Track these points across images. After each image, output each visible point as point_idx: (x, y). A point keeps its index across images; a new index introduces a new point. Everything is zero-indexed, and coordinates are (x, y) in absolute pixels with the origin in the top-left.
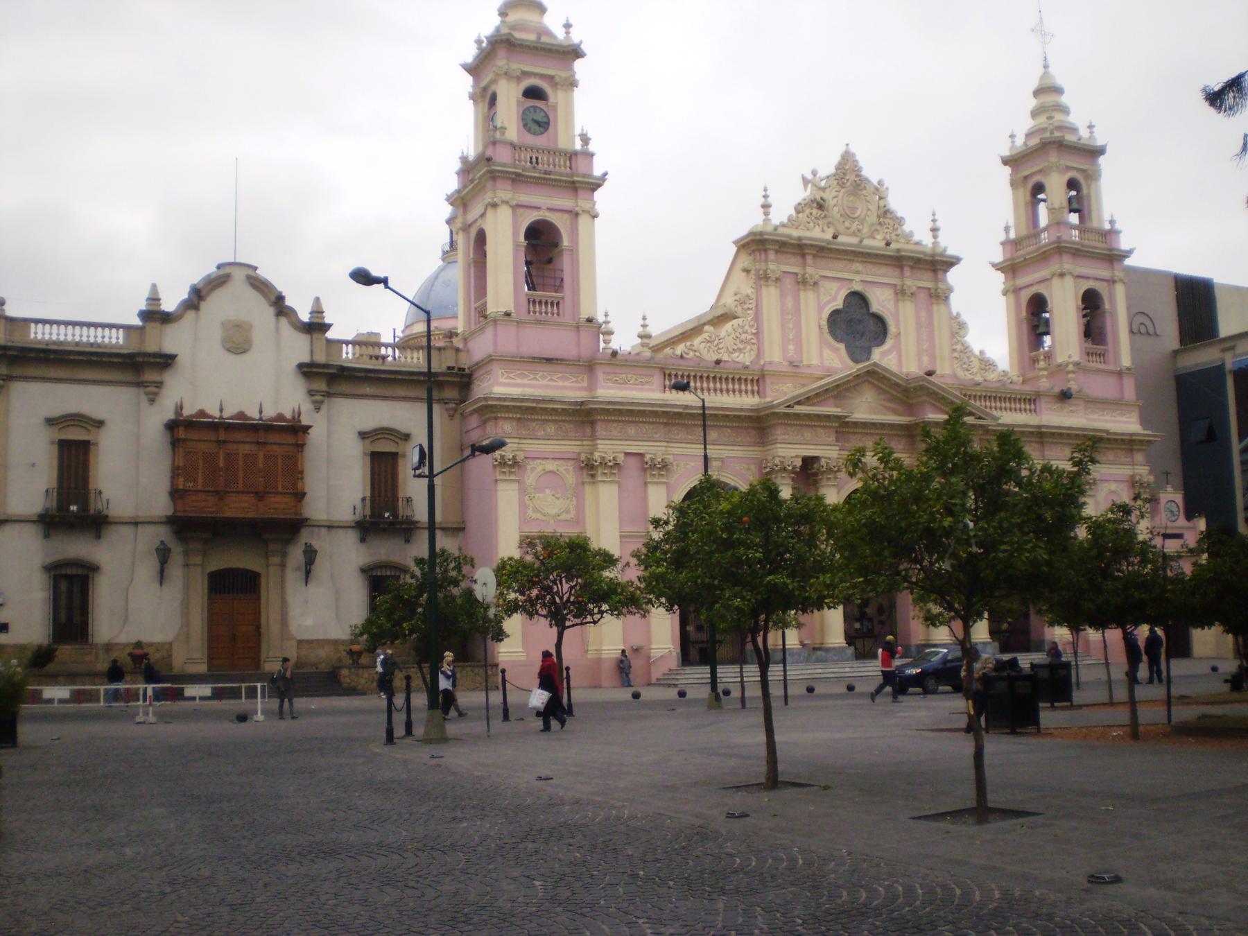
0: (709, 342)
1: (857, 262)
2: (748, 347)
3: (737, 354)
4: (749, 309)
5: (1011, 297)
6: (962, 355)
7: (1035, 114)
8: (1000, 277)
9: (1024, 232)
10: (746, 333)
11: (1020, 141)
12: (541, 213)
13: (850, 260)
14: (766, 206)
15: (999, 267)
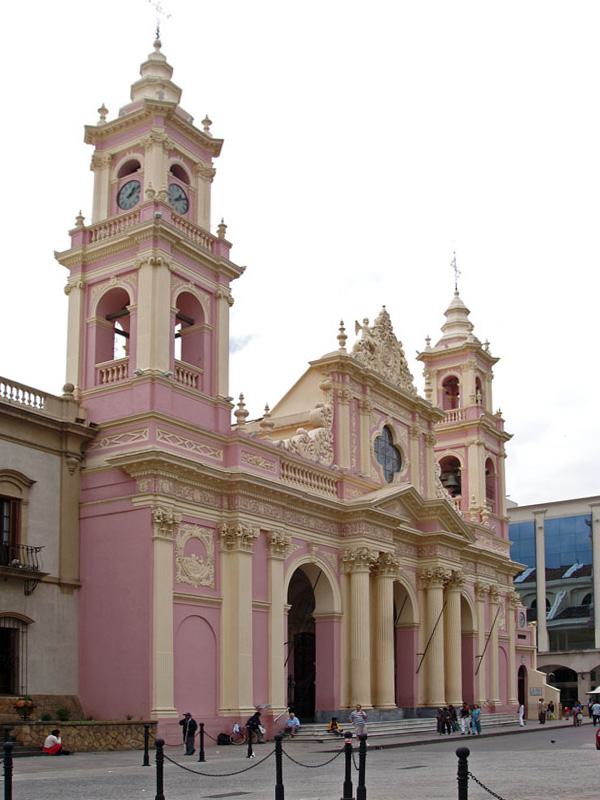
5: (77, 293)
7: (136, 88)
8: (64, 272)
9: (104, 216)
11: (112, 116)
15: (62, 258)
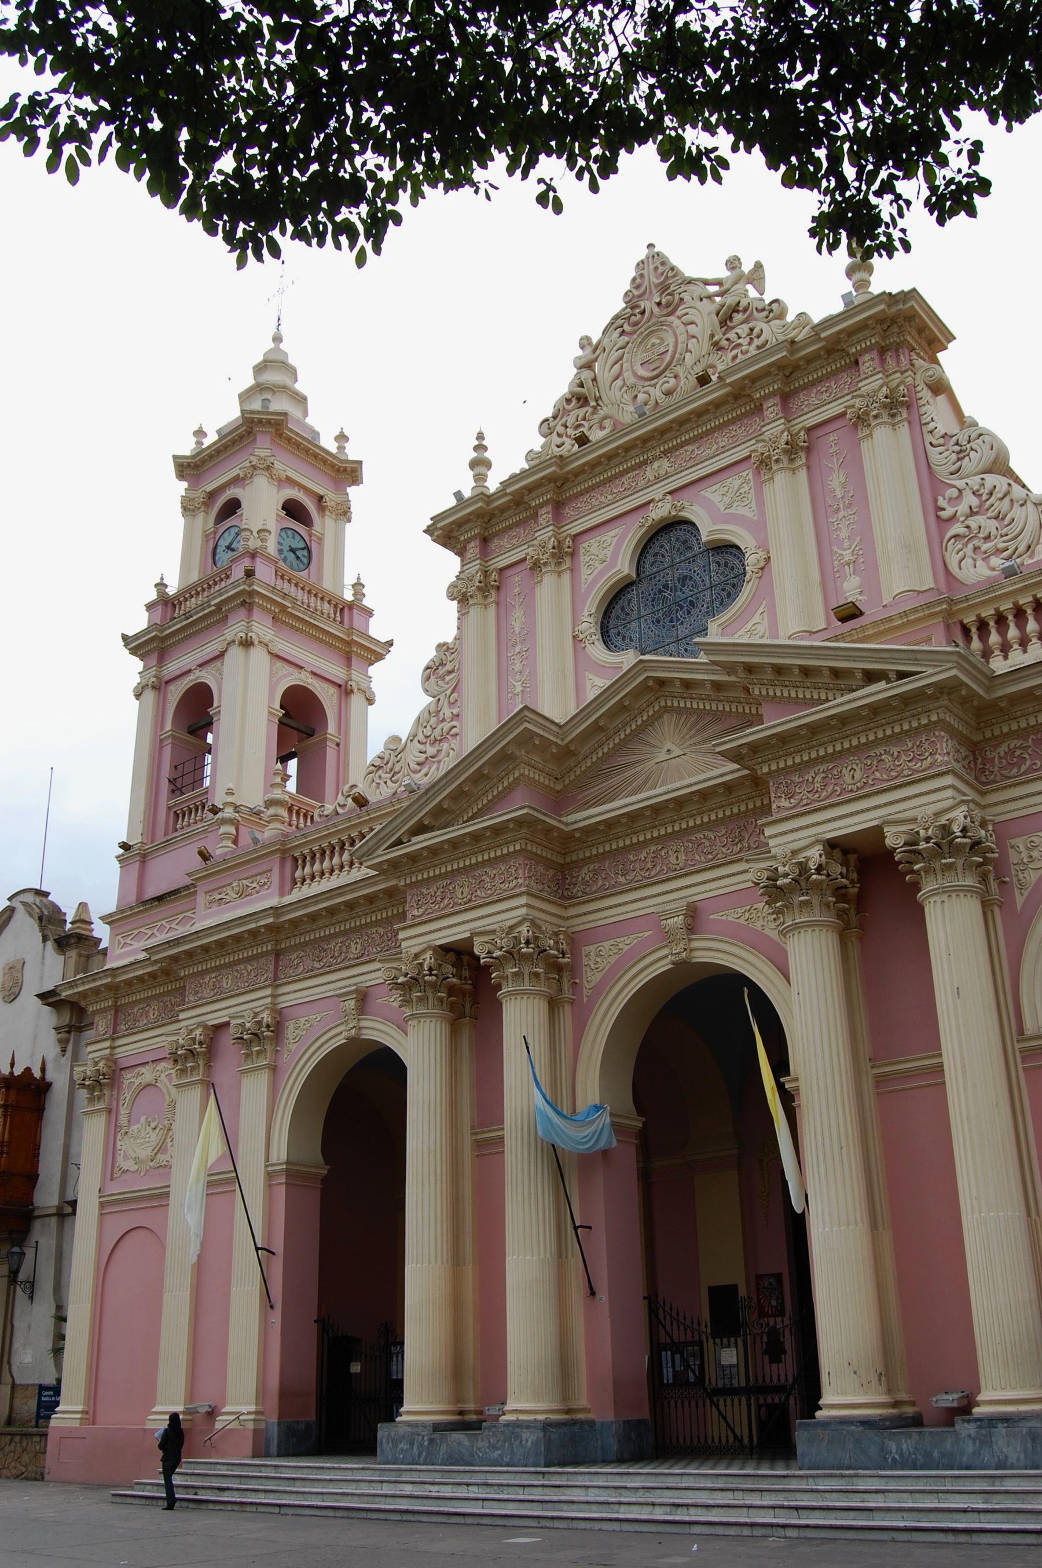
0: (380, 767)
1: (656, 458)
2: (445, 746)
3: (425, 770)
4: (450, 672)
6: (973, 522)
10: (444, 720)
12: (192, 677)
13: (640, 466)
14: (480, 464)
